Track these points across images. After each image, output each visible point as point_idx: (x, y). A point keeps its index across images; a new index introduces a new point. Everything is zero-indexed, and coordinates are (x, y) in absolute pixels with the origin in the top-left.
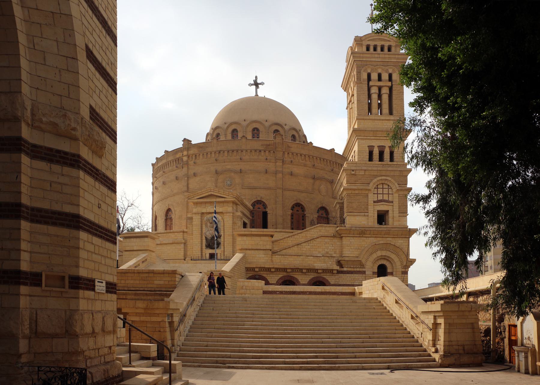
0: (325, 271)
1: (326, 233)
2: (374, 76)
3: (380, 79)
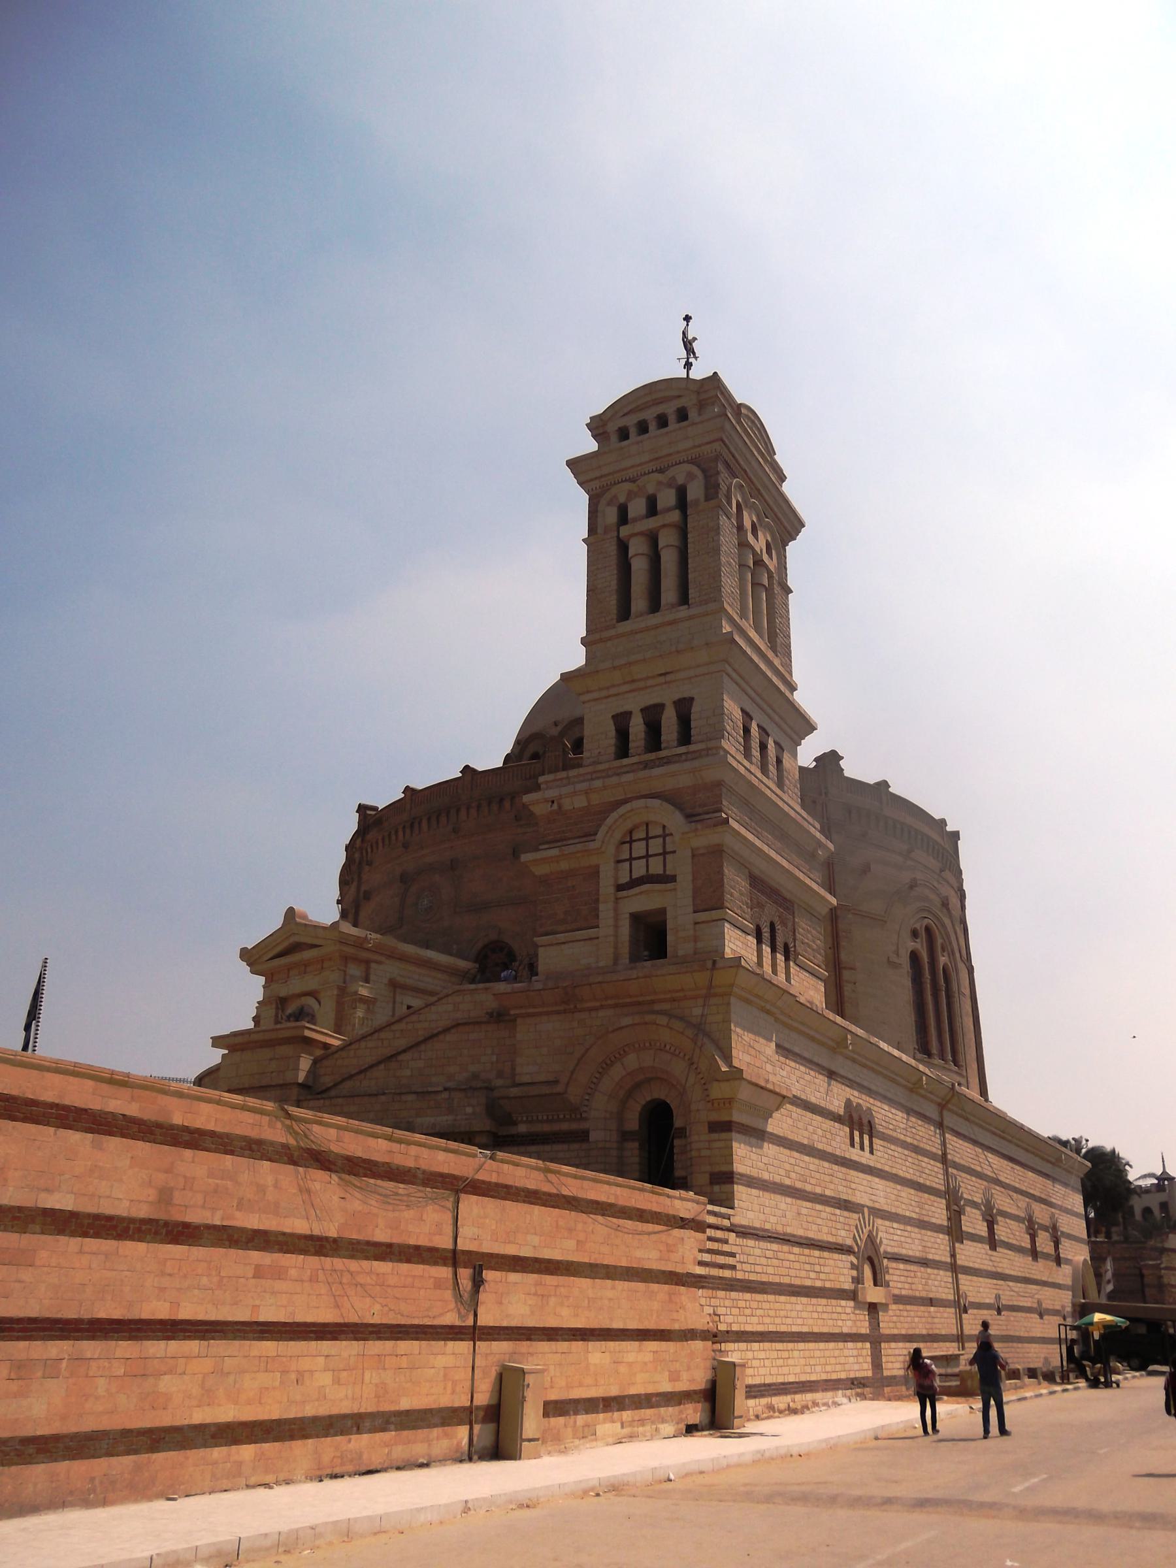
2: (637, 507)
3: (652, 509)
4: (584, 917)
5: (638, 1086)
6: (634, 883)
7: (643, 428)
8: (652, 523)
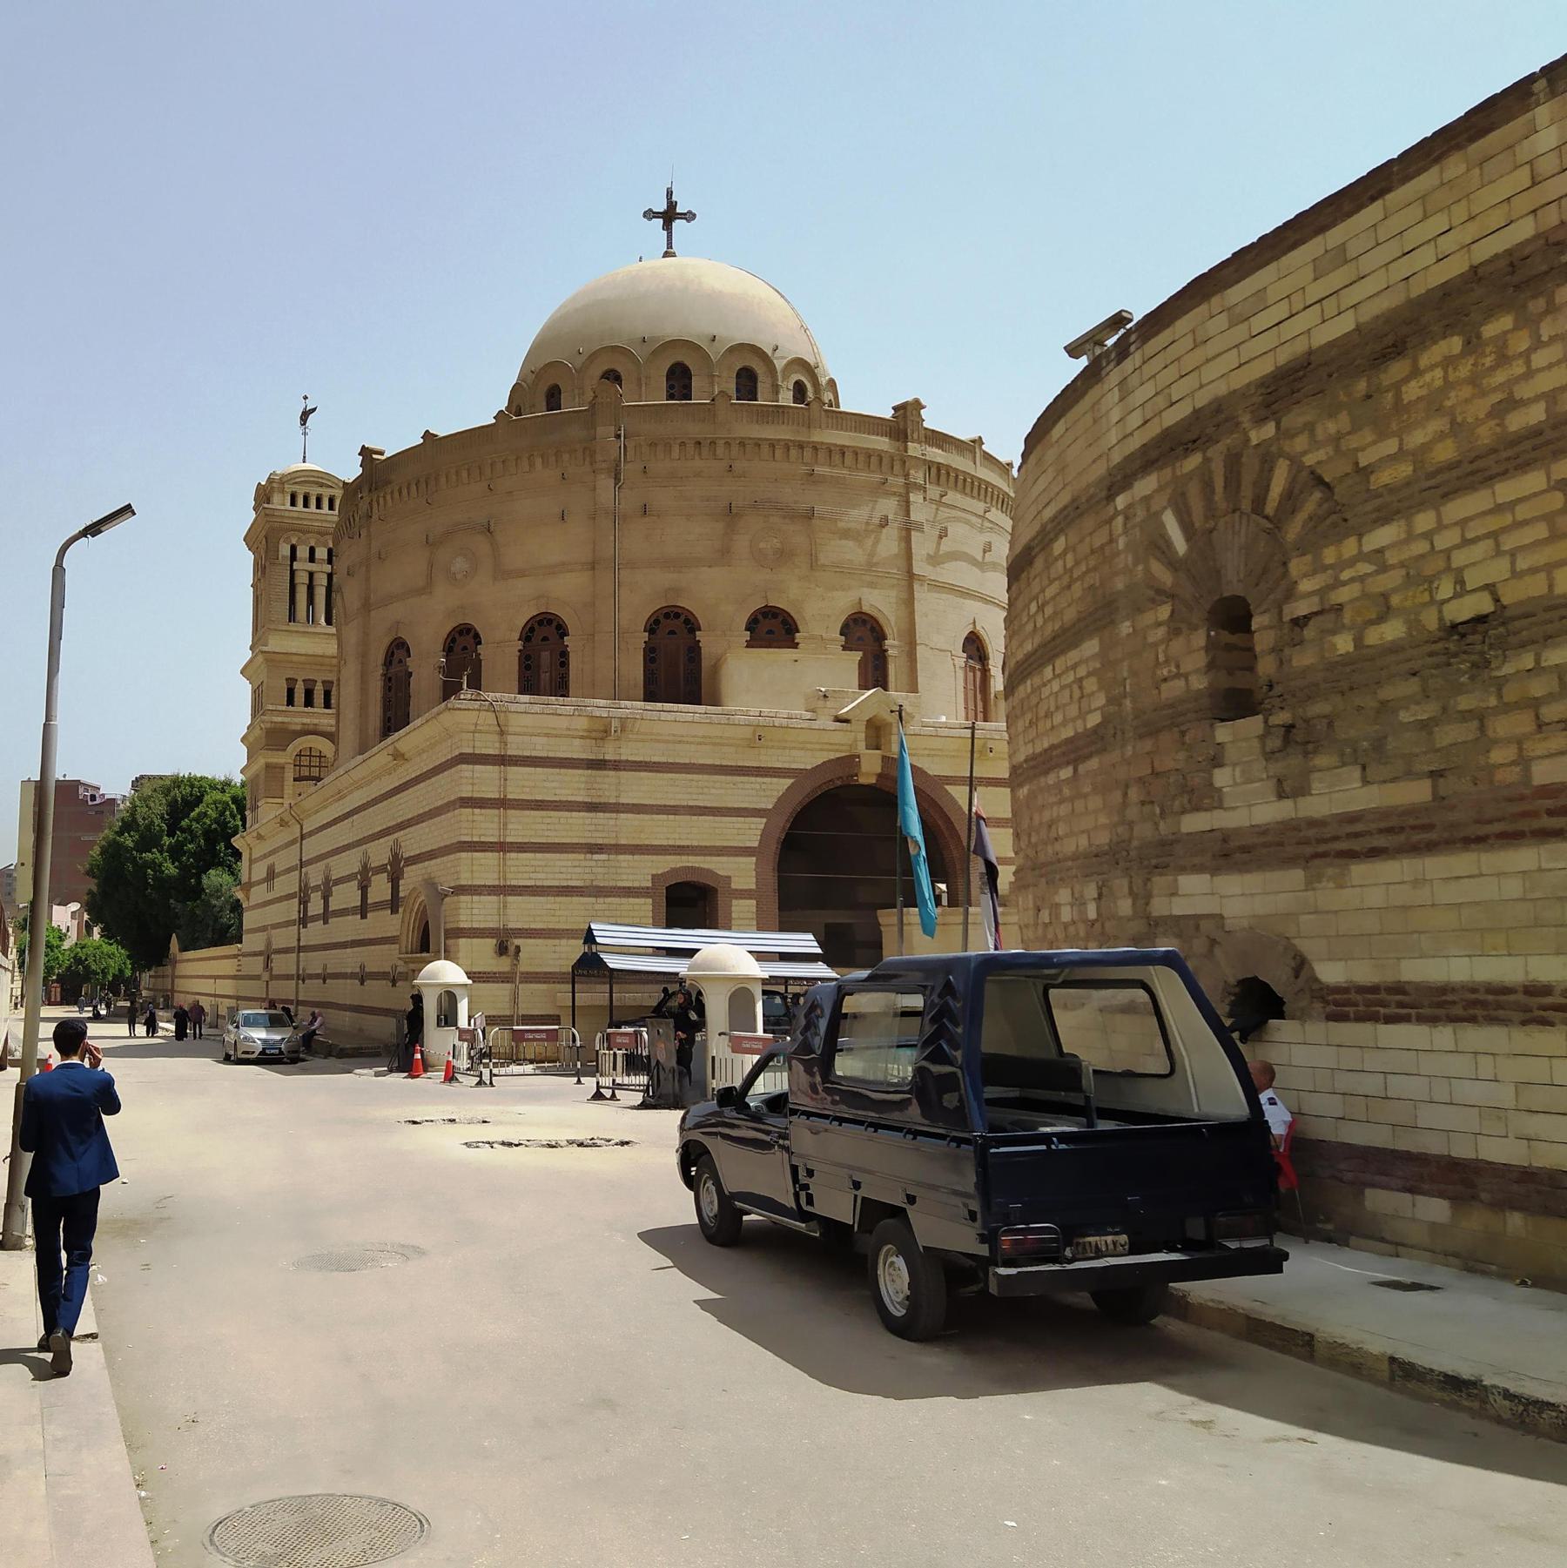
2: (302, 552)
3: (312, 559)
8: (312, 567)
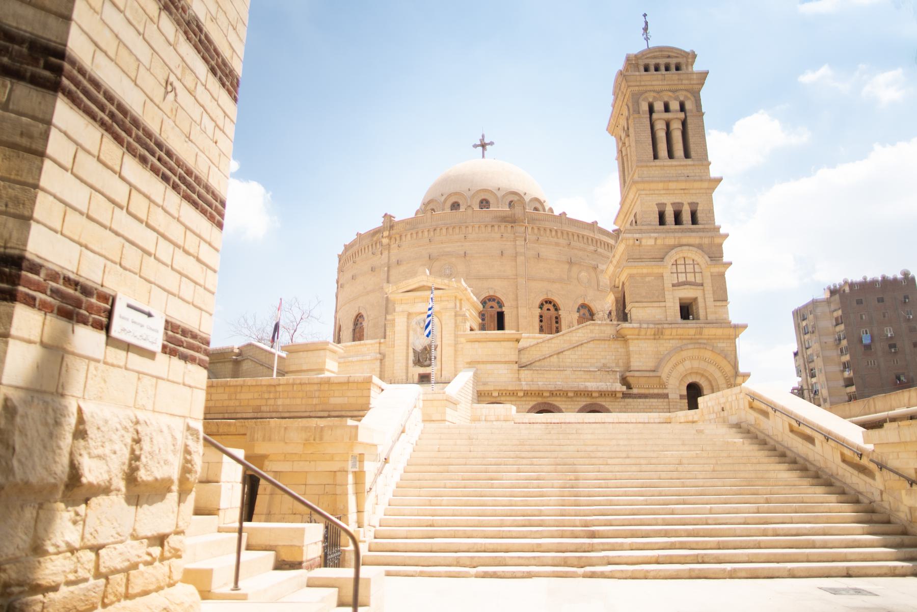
0: (602, 394)
1: (602, 335)
2: (659, 106)
3: (667, 109)
4: (660, 298)
5: (703, 375)
6: (679, 284)
7: (667, 68)
